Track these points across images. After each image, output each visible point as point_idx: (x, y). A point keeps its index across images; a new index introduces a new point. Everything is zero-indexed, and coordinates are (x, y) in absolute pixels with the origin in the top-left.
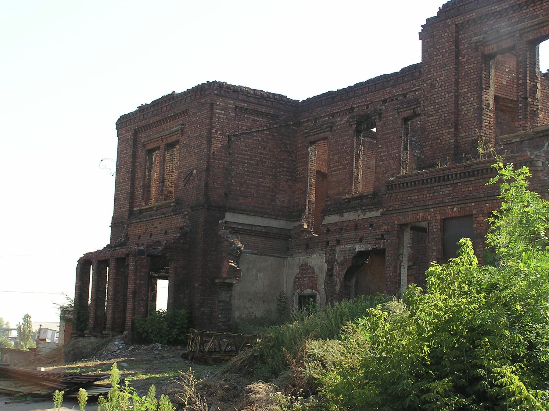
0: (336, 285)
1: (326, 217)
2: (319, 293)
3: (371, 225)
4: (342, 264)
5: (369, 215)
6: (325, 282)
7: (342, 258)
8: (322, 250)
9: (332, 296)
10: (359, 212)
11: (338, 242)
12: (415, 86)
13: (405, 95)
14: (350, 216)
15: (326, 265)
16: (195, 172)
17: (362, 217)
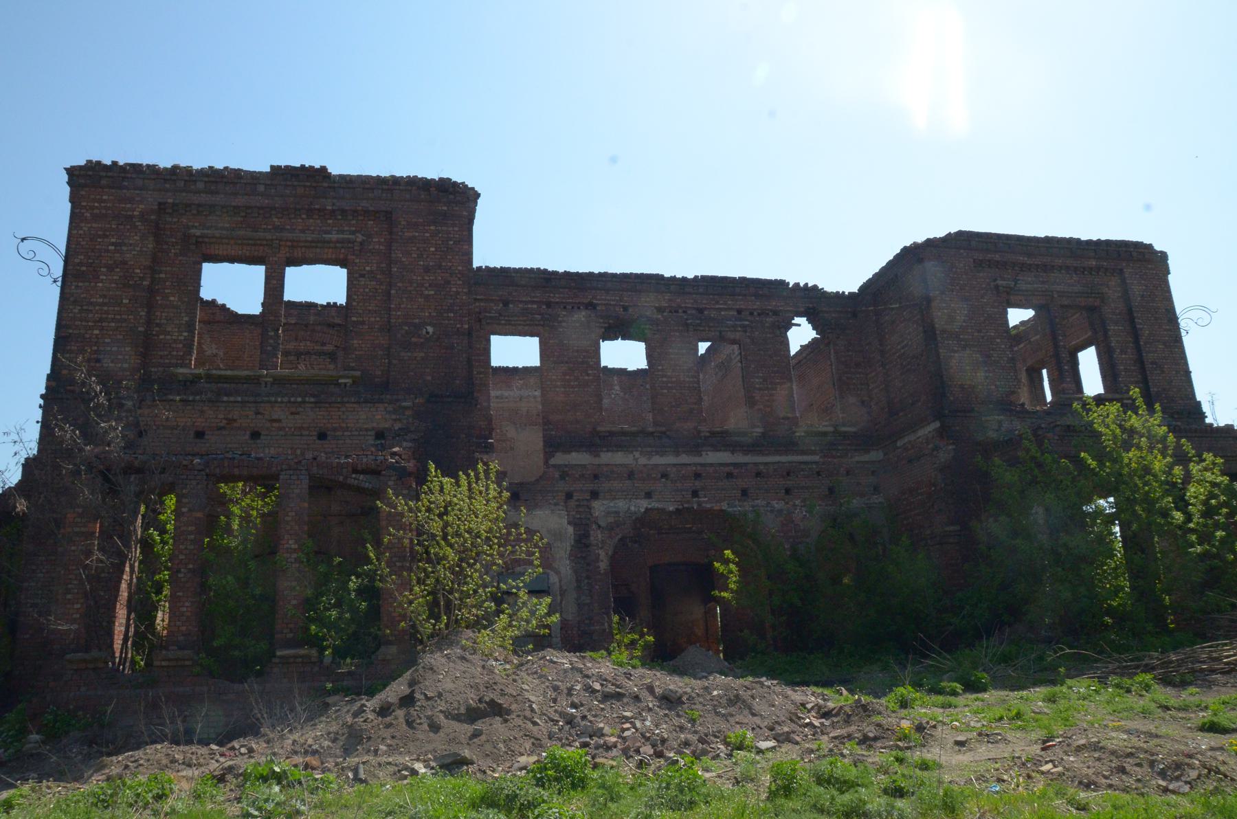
0: (597, 559)
1: (559, 455)
2: (558, 573)
3: (665, 476)
4: (611, 528)
5: (657, 460)
6: (571, 555)
7: (611, 520)
8: (556, 504)
9: (588, 577)
10: (637, 454)
11: (595, 495)
12: (717, 303)
13: (701, 311)
14: (618, 458)
15: (571, 529)
16: (430, 329)
17: (643, 461)
